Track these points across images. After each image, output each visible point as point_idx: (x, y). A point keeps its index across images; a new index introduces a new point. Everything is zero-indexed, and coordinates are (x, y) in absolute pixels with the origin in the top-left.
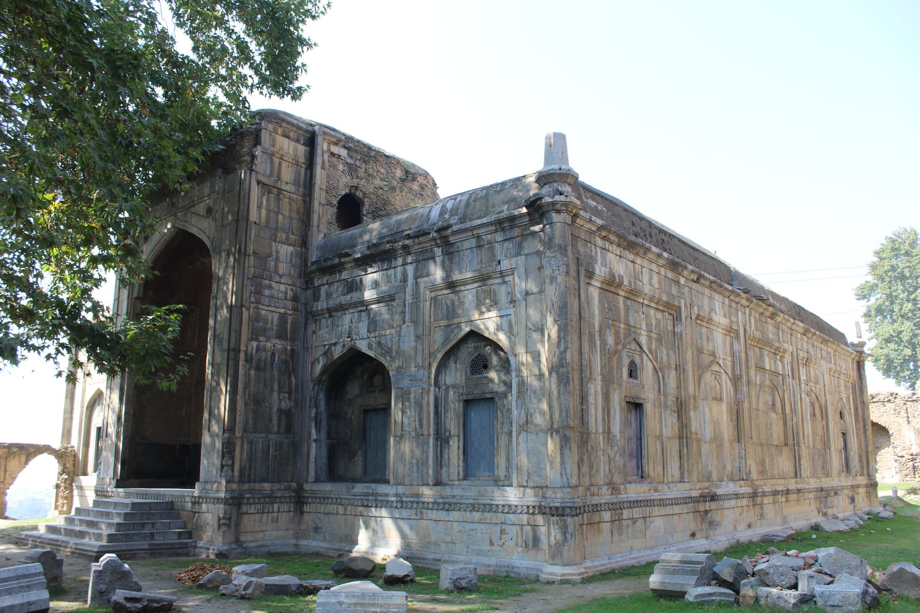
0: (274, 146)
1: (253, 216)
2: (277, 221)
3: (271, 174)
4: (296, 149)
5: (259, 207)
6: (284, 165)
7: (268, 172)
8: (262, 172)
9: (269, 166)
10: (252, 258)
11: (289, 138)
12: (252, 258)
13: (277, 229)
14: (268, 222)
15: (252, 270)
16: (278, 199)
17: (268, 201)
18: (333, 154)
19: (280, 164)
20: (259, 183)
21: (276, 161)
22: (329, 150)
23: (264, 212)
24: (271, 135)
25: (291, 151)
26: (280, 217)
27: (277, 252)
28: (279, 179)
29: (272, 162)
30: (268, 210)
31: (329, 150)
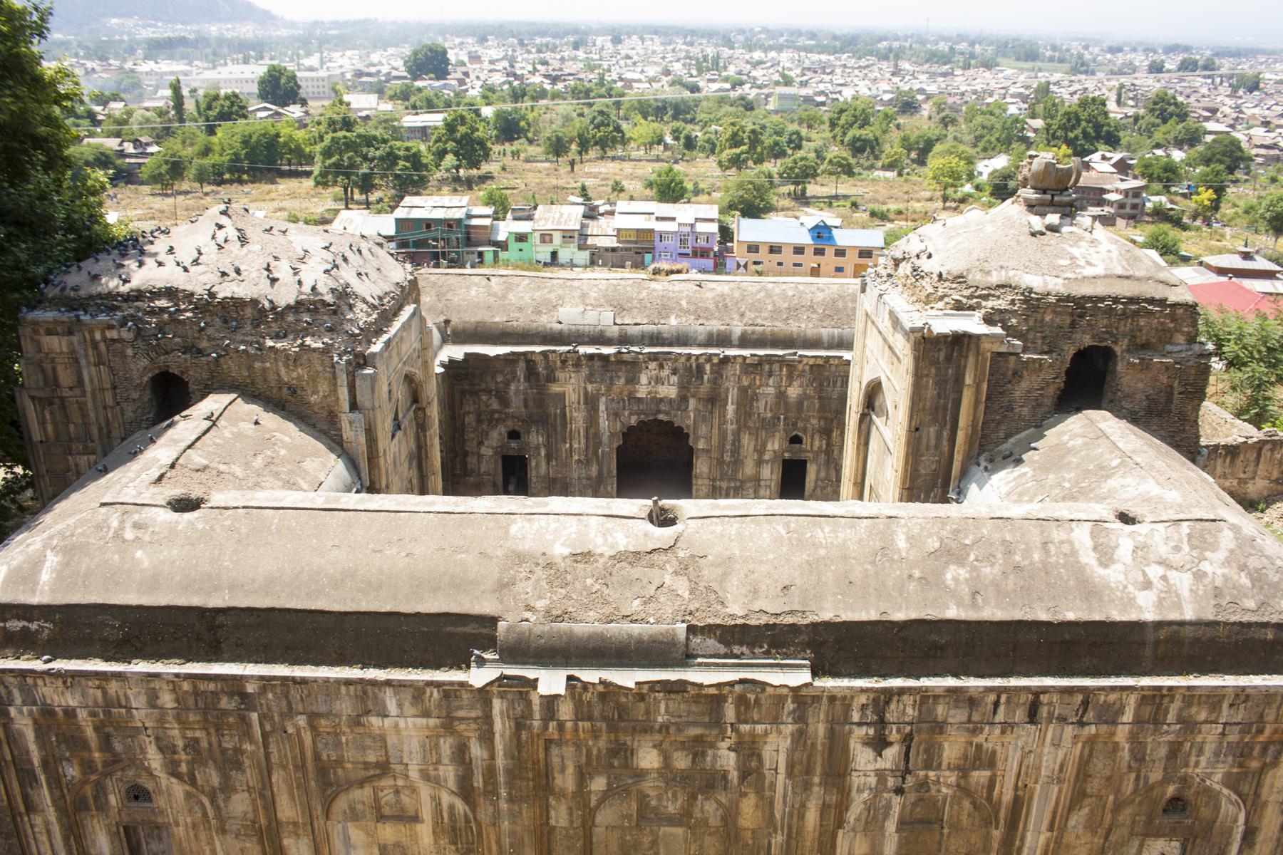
0: (40, 351)
1: (37, 434)
2: (69, 433)
3: (46, 384)
4: (70, 344)
5: (42, 423)
6: (60, 369)
7: (41, 383)
8: (32, 385)
9: (40, 377)
10: (47, 479)
11: (57, 334)
12: (47, 479)
13: (70, 440)
14: (57, 436)
15: (51, 489)
16: (63, 406)
17: (51, 413)
18: (113, 340)
19: (54, 369)
20: (33, 398)
21: (48, 367)
22: (105, 339)
23: (50, 428)
24: (32, 339)
25: (65, 349)
26: (72, 427)
27: (77, 465)
28: (58, 385)
29: (43, 371)
30: (55, 423)
31: (105, 339)
